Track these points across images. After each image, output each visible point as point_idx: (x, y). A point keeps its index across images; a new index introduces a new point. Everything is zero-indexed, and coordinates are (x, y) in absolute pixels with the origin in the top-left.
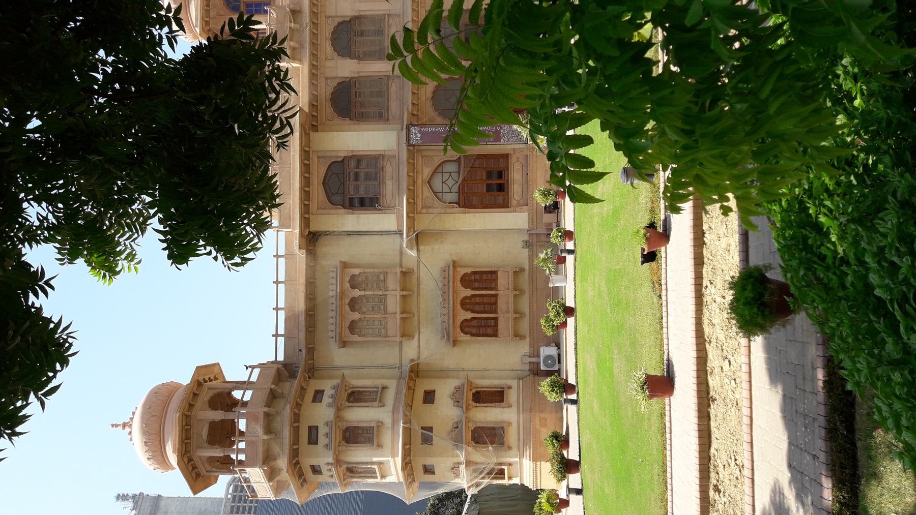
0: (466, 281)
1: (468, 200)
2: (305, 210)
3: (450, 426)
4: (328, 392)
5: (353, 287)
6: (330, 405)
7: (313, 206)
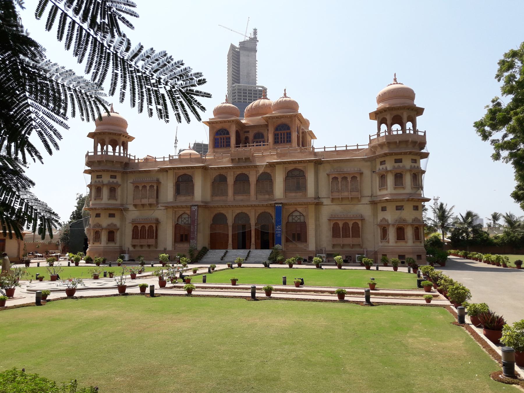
0: (151, 227)
1: (177, 227)
2: (174, 168)
3: (100, 223)
4: (115, 180)
5: (150, 186)
6: (109, 181)
7: (175, 171)
